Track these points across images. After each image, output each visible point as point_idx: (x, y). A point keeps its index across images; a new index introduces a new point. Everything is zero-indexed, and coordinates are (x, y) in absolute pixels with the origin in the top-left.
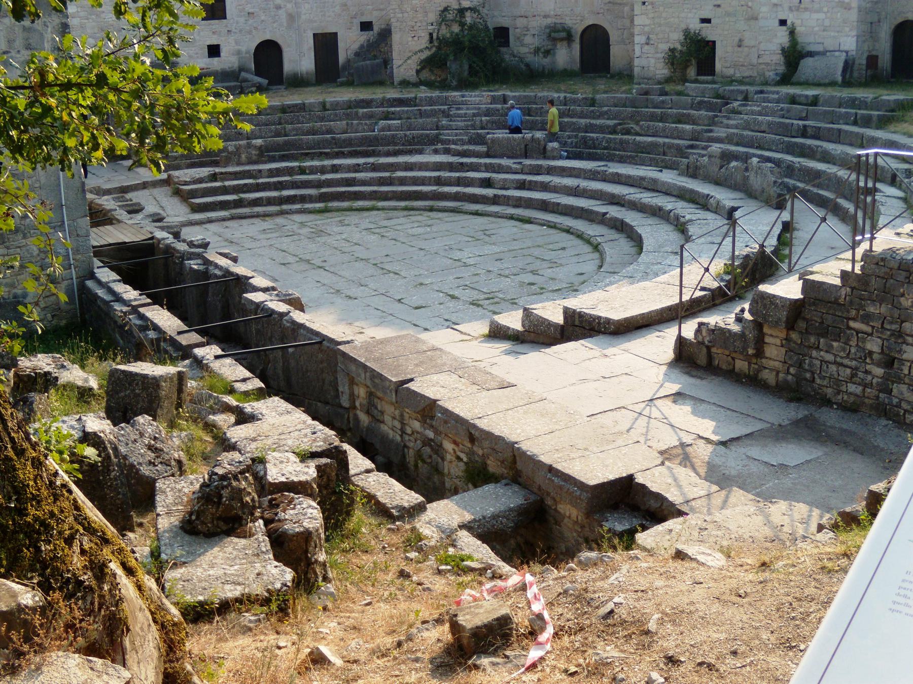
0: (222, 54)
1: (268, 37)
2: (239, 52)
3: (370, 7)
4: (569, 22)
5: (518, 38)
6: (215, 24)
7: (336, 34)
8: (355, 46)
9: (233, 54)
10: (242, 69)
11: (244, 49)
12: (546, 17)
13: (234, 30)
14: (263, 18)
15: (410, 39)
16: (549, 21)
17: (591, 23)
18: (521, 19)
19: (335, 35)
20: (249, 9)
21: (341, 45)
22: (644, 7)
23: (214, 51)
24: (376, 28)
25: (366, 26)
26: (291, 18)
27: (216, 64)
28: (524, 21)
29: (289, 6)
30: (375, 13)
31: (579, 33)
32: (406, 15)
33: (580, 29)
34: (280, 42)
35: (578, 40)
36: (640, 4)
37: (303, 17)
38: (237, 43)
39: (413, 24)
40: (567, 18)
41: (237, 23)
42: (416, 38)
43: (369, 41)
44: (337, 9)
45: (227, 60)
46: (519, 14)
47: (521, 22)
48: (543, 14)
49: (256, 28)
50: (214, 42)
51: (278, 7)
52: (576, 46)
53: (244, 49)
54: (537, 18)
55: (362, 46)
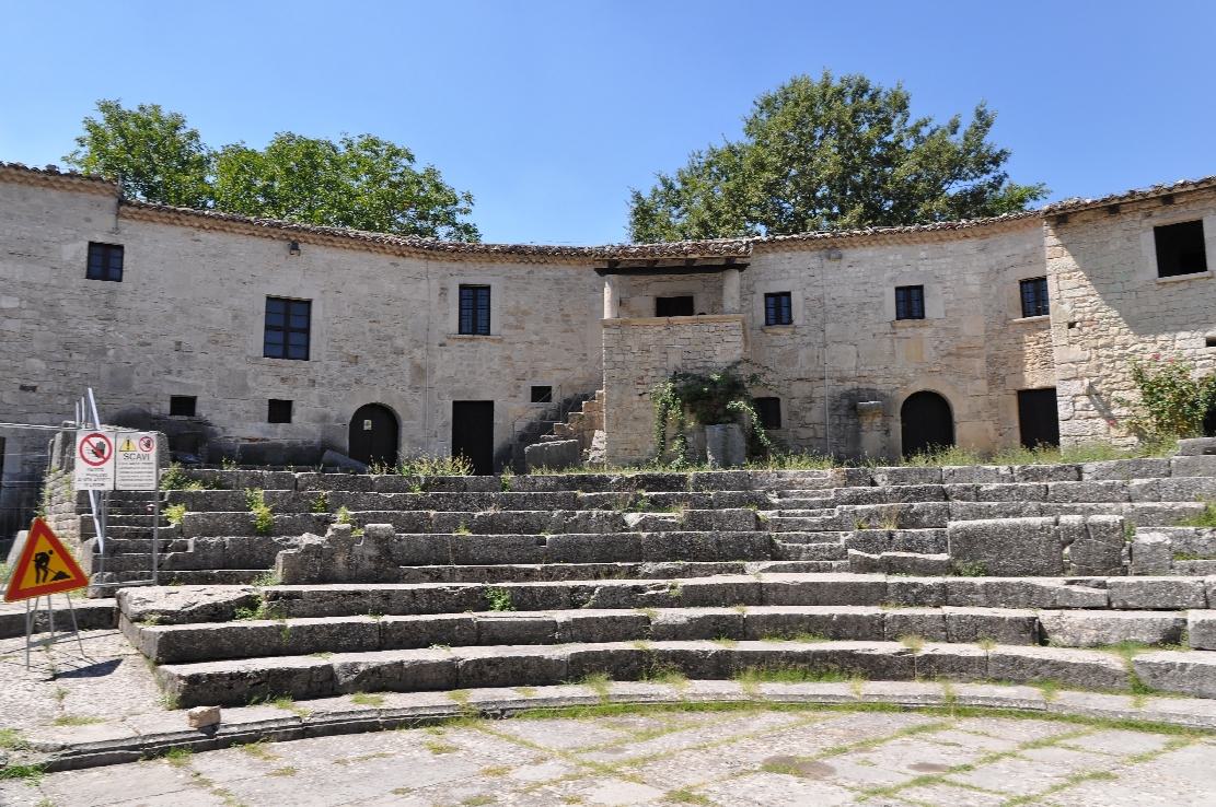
0: (294, 418)
1: (377, 398)
2: (324, 418)
3: (548, 364)
4: (880, 385)
5: (796, 414)
6: (288, 366)
7: (491, 403)
8: (520, 426)
9: (314, 421)
10: (326, 445)
11: (334, 414)
12: (842, 380)
13: (319, 379)
14: (372, 366)
15: (637, 398)
16: (848, 386)
17: (920, 388)
18: (800, 384)
19: (491, 403)
20: (349, 348)
21: (498, 420)
22: (1073, 332)
23: (280, 411)
24: (557, 397)
25: (540, 394)
26: (420, 372)
27: (279, 434)
28: (805, 388)
29: (418, 354)
30: (557, 375)
31: (900, 405)
32: (630, 357)
33: (903, 395)
34: (398, 408)
35: (898, 416)
36: (1066, 325)
37: (439, 373)
38: (323, 401)
39: (643, 373)
40: (879, 381)
41: (327, 369)
42: (646, 397)
43: (543, 418)
44: (496, 365)
45: (304, 427)
46: (796, 375)
47: (799, 389)
48: (838, 375)
49: (358, 382)
50: (282, 394)
51: (399, 352)
52: (897, 426)
53: (334, 414)
54: (827, 381)
55: (531, 425)
